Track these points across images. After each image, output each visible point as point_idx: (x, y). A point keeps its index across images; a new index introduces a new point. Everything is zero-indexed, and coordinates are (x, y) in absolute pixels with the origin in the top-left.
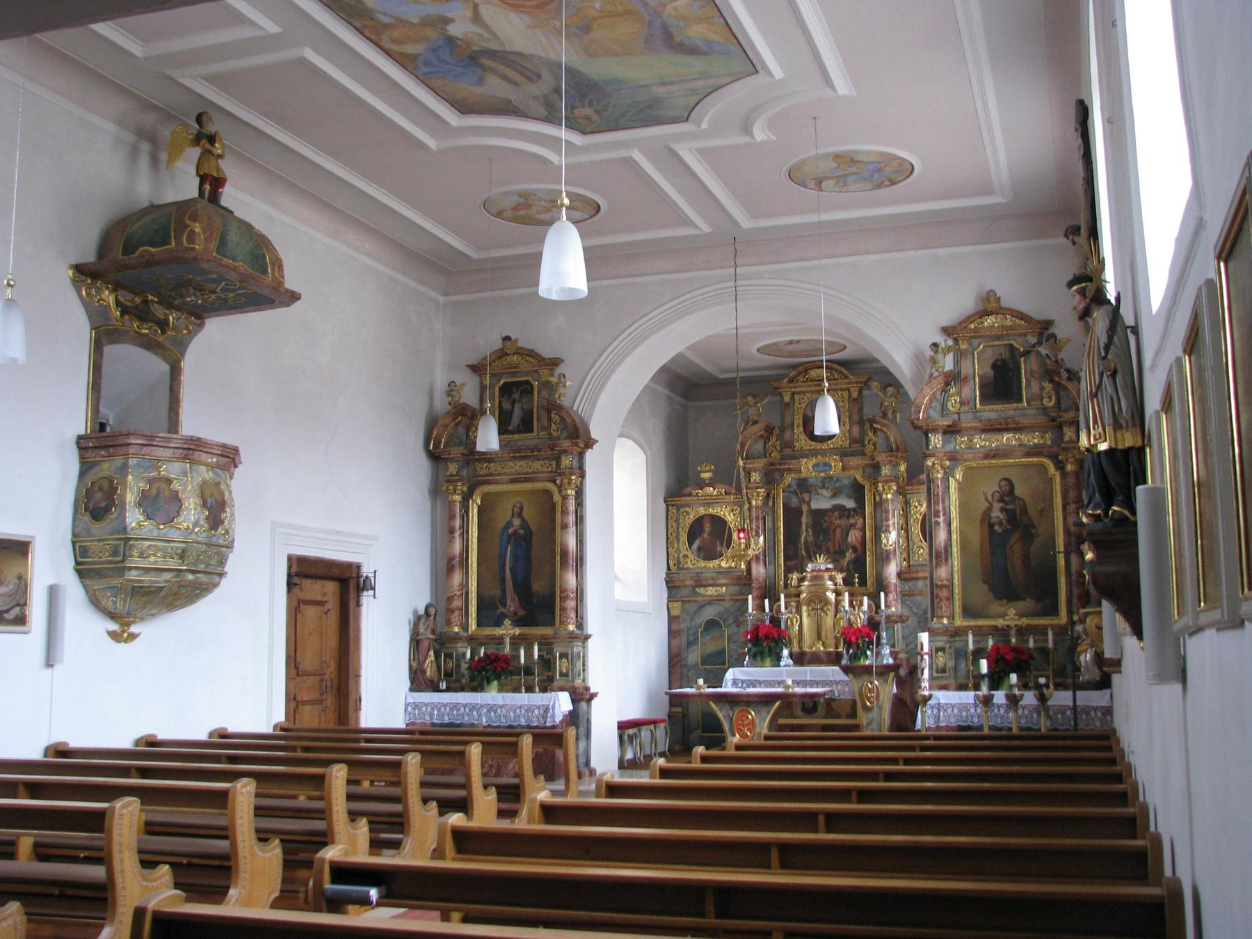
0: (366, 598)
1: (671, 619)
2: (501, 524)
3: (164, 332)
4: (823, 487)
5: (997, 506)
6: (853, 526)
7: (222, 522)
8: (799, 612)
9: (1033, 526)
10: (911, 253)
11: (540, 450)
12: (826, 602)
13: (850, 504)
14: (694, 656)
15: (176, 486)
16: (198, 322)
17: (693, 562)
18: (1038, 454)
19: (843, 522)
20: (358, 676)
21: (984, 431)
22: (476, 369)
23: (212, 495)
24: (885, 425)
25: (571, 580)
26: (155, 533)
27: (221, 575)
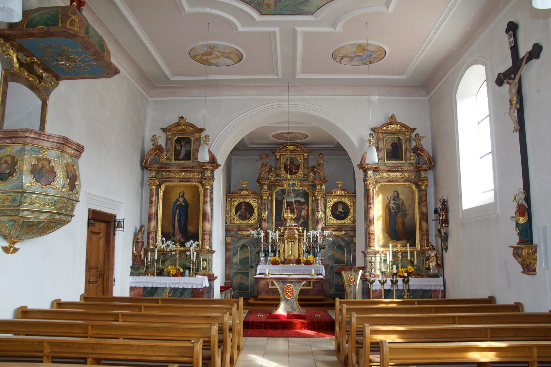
0: (119, 232)
1: (227, 244)
2: (174, 200)
3: (40, 82)
5: (392, 202)
6: (304, 209)
7: (75, 187)
8: (283, 243)
9: (406, 211)
10: (359, 97)
11: (194, 168)
12: (295, 238)
13: (302, 200)
14: (236, 259)
15: (53, 164)
16: (56, 82)
17: (237, 221)
18: (409, 182)
20: (113, 269)
21: (388, 171)
22: (164, 130)
23: (71, 172)
24: (319, 169)
25: (207, 225)
26: (40, 190)
27: (72, 216)
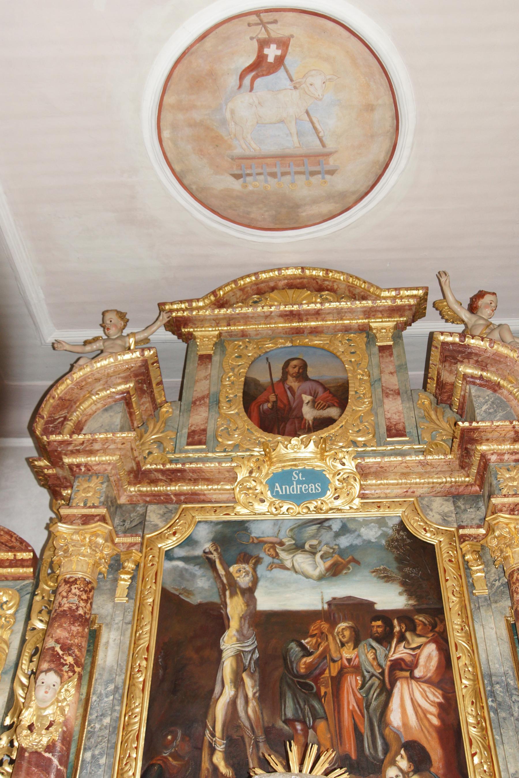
4: (298, 547)
6: (403, 668)
13: (390, 598)
19: (368, 655)
